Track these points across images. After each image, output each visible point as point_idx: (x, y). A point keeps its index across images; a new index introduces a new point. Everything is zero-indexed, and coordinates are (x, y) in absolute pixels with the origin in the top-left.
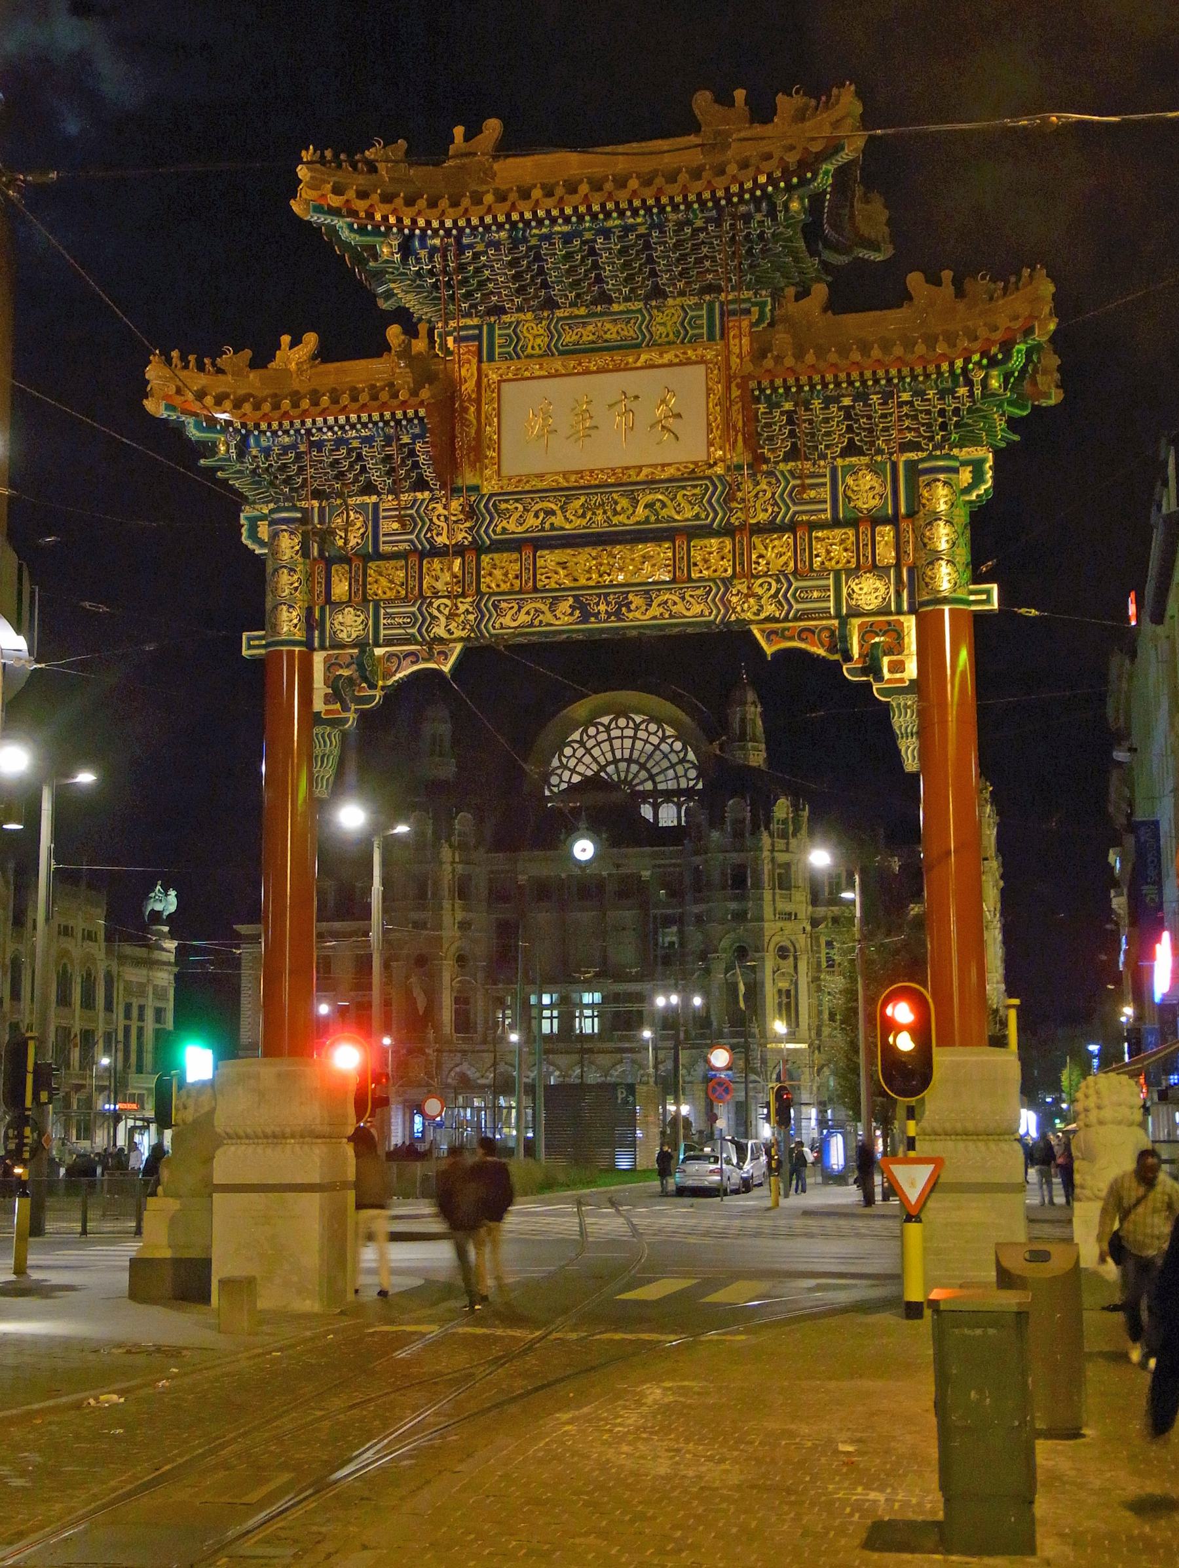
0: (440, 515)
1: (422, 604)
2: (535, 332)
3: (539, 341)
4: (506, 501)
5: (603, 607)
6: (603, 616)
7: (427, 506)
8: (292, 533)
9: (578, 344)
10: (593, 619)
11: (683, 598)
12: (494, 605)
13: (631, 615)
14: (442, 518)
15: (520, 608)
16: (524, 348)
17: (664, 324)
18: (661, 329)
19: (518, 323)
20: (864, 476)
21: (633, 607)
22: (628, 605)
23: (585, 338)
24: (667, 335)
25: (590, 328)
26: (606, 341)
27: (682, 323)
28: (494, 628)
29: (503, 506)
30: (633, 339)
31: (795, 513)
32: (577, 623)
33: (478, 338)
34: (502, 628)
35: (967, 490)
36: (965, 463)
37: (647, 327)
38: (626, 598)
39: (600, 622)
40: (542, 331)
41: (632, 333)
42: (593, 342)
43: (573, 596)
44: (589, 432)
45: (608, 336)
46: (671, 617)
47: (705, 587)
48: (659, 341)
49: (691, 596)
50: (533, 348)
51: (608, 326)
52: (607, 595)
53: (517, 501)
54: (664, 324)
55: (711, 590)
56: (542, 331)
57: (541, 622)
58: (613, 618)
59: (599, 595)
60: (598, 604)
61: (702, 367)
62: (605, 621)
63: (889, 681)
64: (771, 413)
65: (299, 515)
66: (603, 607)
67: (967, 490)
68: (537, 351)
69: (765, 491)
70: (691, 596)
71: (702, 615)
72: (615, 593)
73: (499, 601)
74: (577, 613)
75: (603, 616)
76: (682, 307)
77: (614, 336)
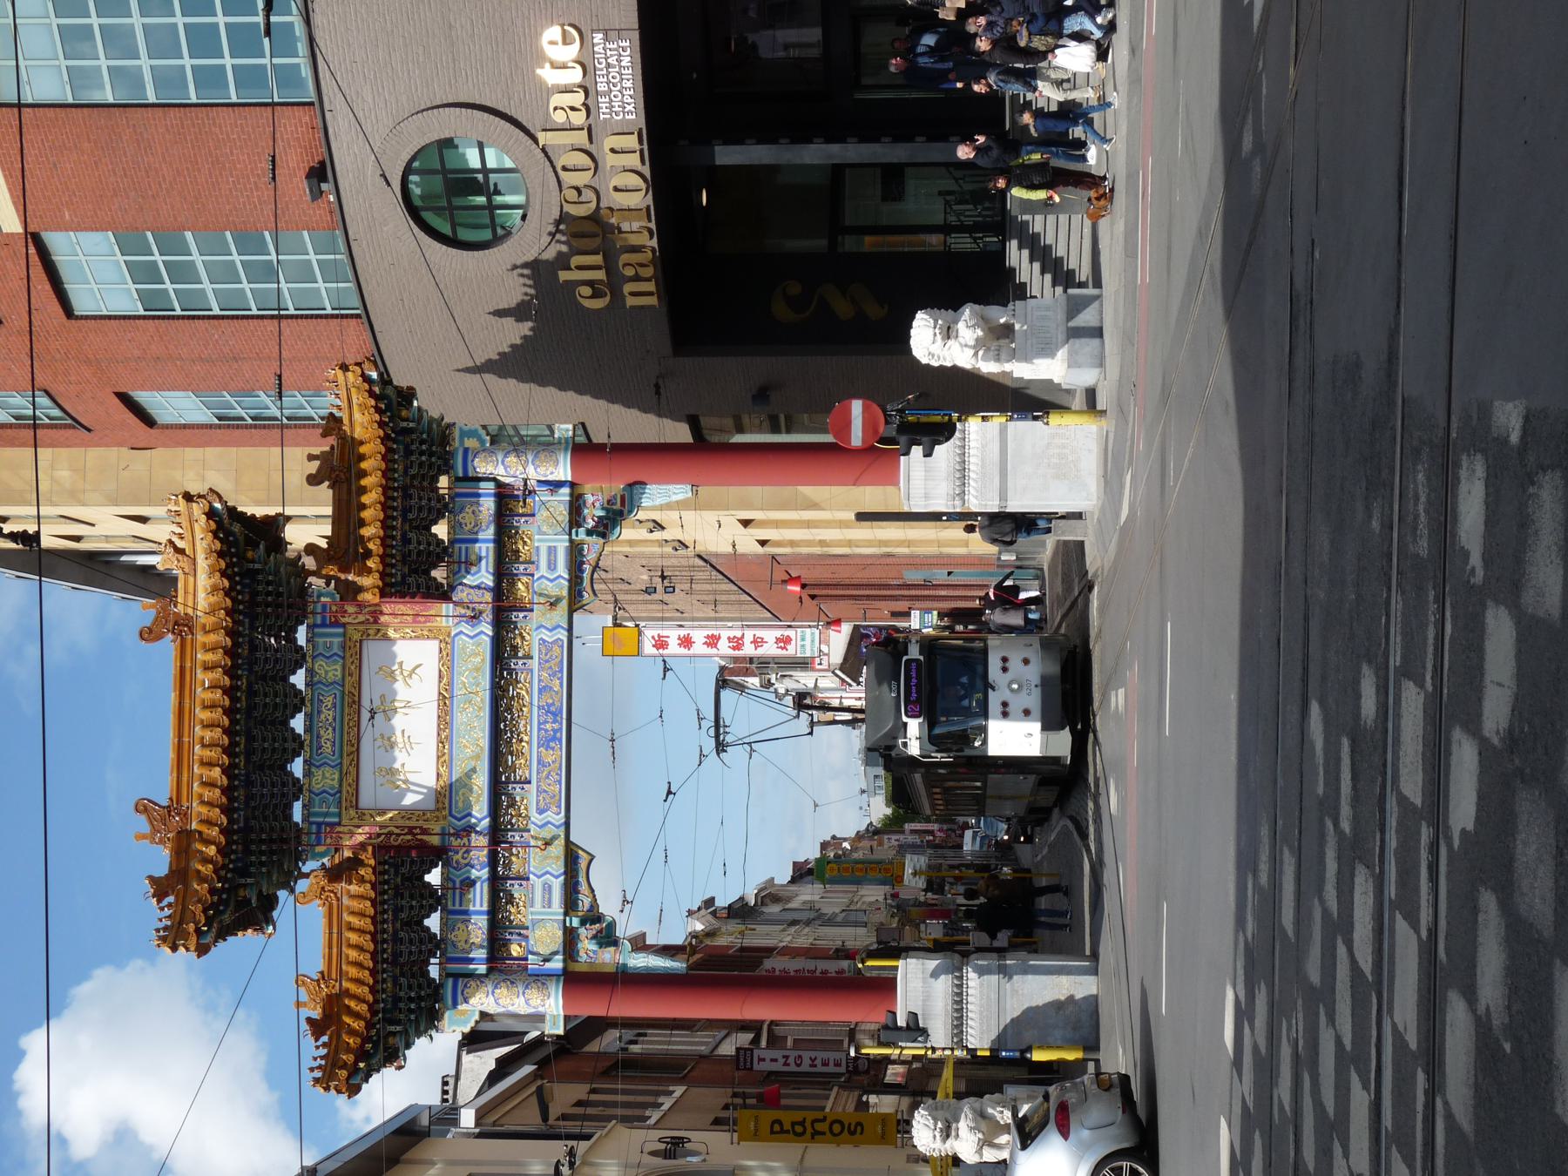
0: (463, 858)
1: (535, 875)
2: (320, 778)
3: (327, 775)
4: (457, 802)
5: (548, 726)
6: (556, 726)
7: (454, 868)
8: (465, 986)
9: (334, 742)
10: (558, 735)
11: (547, 661)
12: (540, 813)
13: (559, 704)
14: (466, 855)
15: (545, 791)
16: (332, 787)
17: (326, 672)
18: (330, 674)
19: (310, 791)
20: (463, 518)
21: (550, 701)
22: (549, 705)
23: (330, 736)
24: (336, 670)
25: (322, 732)
26: (334, 719)
27: (328, 658)
28: (558, 814)
29: (460, 804)
30: (335, 698)
31: (487, 571)
32: (561, 745)
33: (319, 825)
34: (560, 807)
35: (482, 442)
36: (462, 442)
37: (327, 686)
38: (543, 707)
39: (561, 729)
40: (320, 772)
41: (331, 698)
42: (334, 729)
43: (538, 748)
44: (406, 735)
45: (330, 718)
46: (561, 671)
47: (540, 644)
48: (340, 676)
49: (546, 655)
50: (333, 780)
51: (323, 716)
52: (539, 724)
53: (457, 794)
54: (326, 672)
55: (541, 639)
56: (320, 772)
57: (557, 774)
58: (559, 719)
59: (539, 729)
60: (546, 731)
61: (365, 643)
62: (561, 724)
63: (623, 503)
64: (409, 584)
65: (450, 982)
66: (548, 726)
67: (482, 442)
68: (336, 776)
69: (468, 594)
70: (546, 655)
71: (562, 646)
72: (539, 716)
73: (537, 809)
74: (552, 744)
75: (556, 726)
76: (314, 658)
77: (331, 713)
